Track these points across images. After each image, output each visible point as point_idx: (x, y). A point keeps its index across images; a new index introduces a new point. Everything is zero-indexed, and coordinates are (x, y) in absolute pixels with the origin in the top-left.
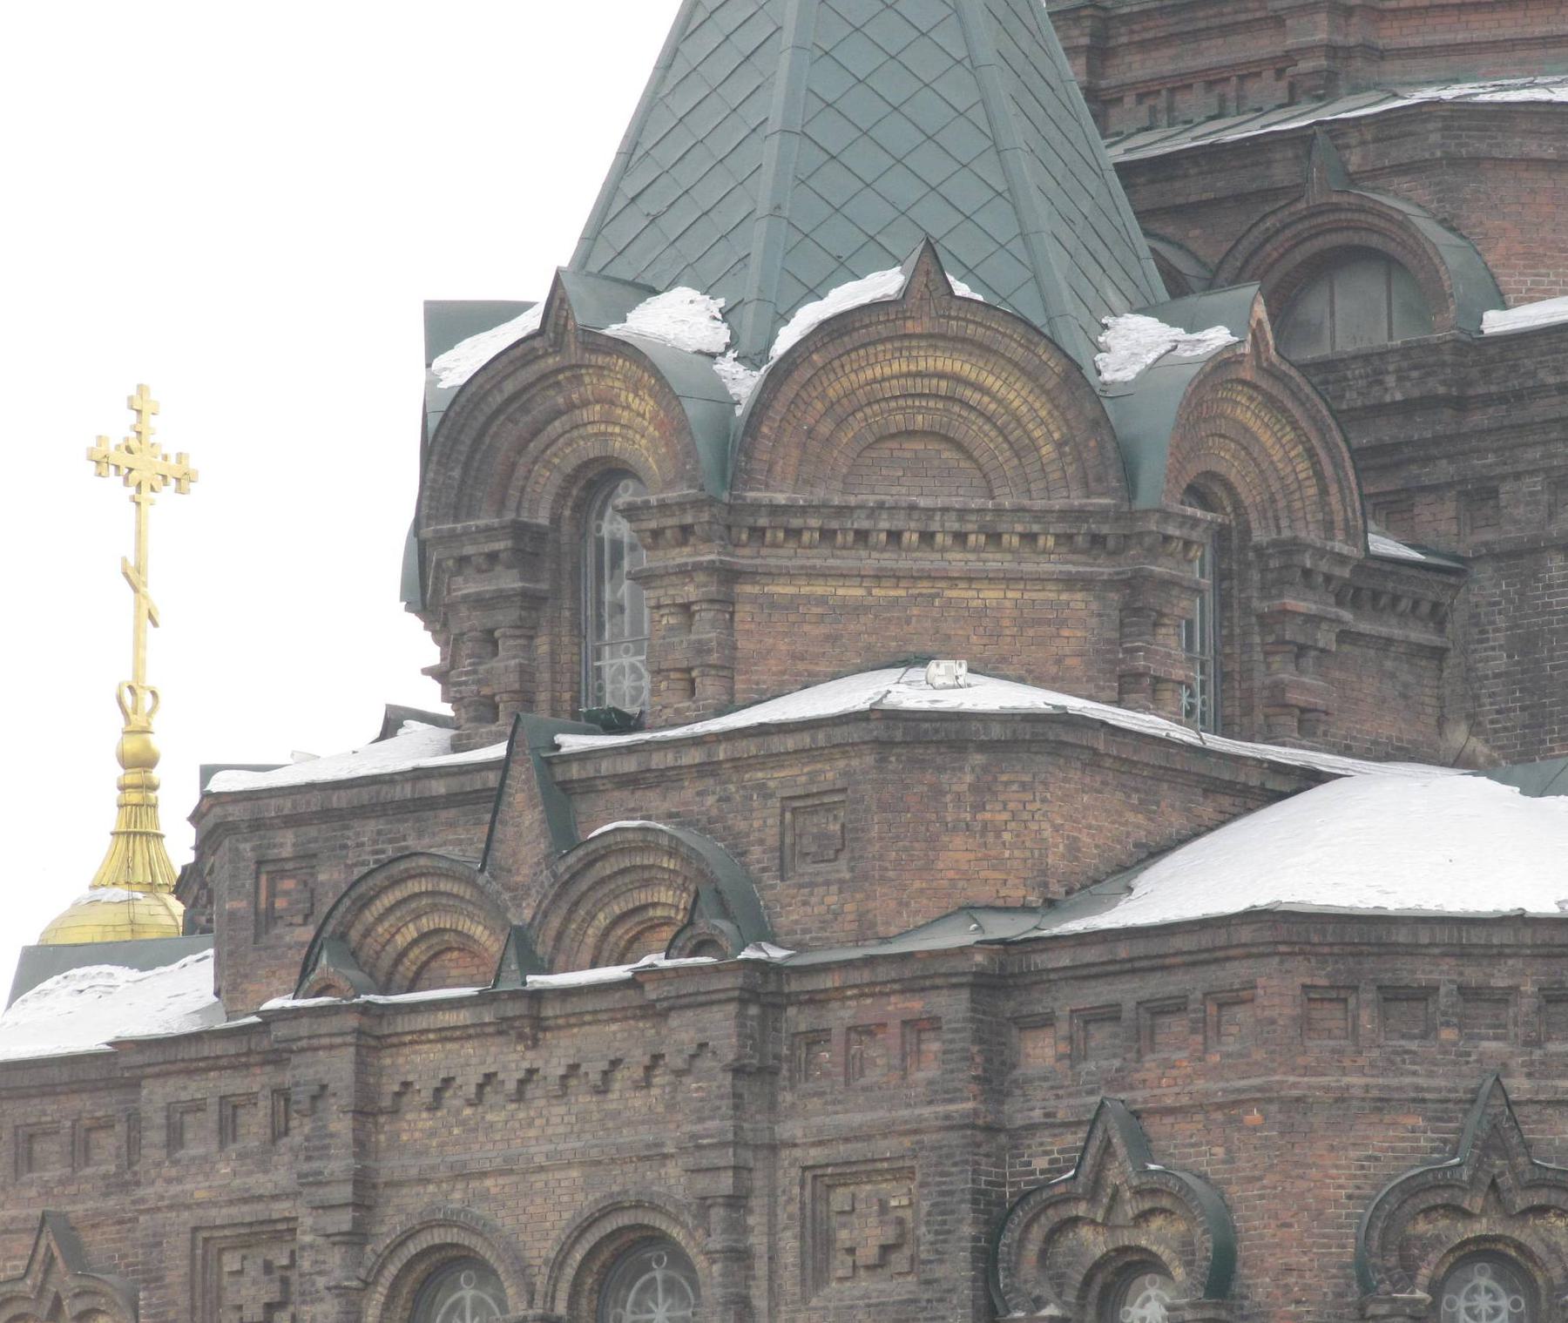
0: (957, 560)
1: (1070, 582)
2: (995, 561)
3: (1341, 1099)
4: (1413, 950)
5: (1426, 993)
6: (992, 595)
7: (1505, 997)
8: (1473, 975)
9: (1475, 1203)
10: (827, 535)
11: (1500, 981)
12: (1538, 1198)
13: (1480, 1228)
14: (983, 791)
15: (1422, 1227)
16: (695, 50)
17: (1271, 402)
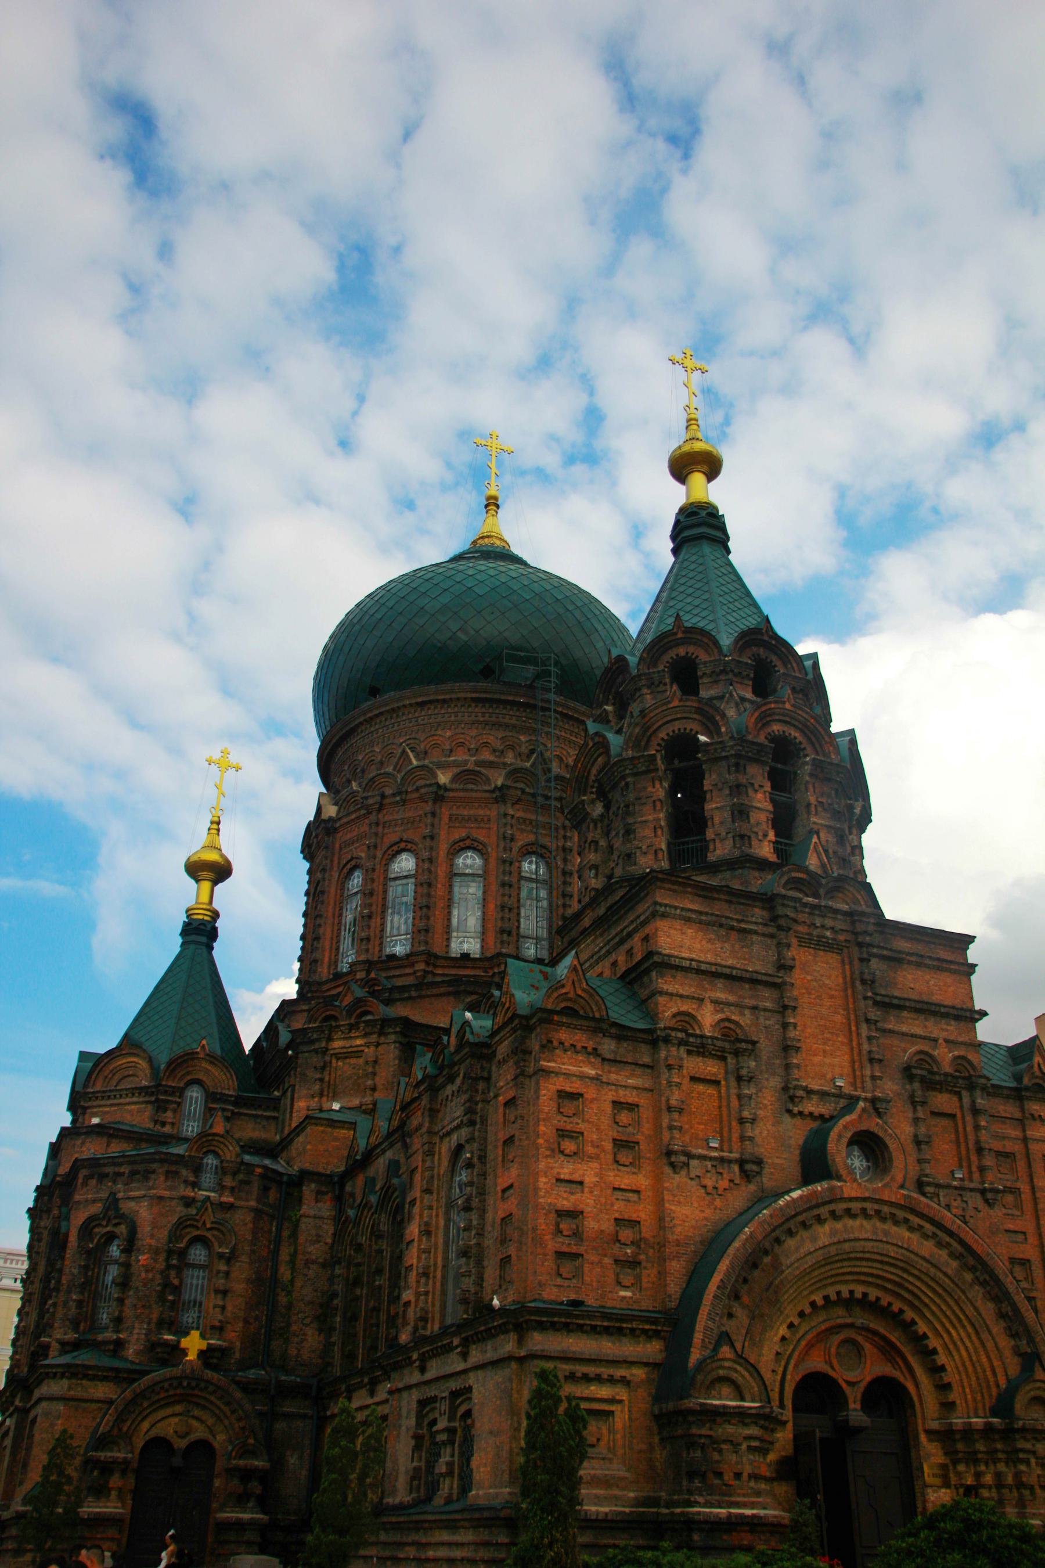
0: (128, 1100)
1: (147, 1102)
2: (135, 1099)
3: (87, 1201)
4: (105, 1165)
5: (107, 1175)
6: (133, 1107)
7: (123, 1174)
8: (117, 1169)
9: (104, 1223)
10: (103, 1098)
11: (122, 1170)
12: (116, 1221)
13: (108, 1229)
14: (83, 1143)
15: (96, 1230)
16: (147, 1009)
17: (211, 1062)
